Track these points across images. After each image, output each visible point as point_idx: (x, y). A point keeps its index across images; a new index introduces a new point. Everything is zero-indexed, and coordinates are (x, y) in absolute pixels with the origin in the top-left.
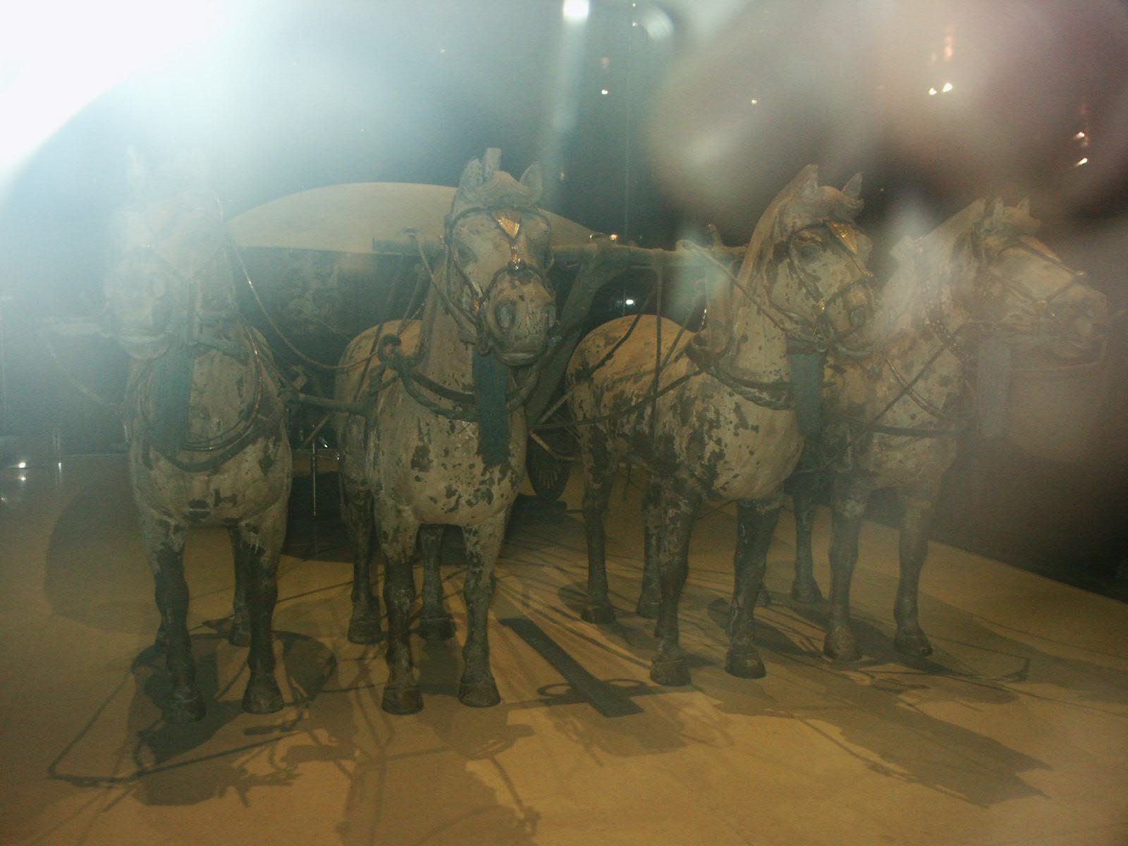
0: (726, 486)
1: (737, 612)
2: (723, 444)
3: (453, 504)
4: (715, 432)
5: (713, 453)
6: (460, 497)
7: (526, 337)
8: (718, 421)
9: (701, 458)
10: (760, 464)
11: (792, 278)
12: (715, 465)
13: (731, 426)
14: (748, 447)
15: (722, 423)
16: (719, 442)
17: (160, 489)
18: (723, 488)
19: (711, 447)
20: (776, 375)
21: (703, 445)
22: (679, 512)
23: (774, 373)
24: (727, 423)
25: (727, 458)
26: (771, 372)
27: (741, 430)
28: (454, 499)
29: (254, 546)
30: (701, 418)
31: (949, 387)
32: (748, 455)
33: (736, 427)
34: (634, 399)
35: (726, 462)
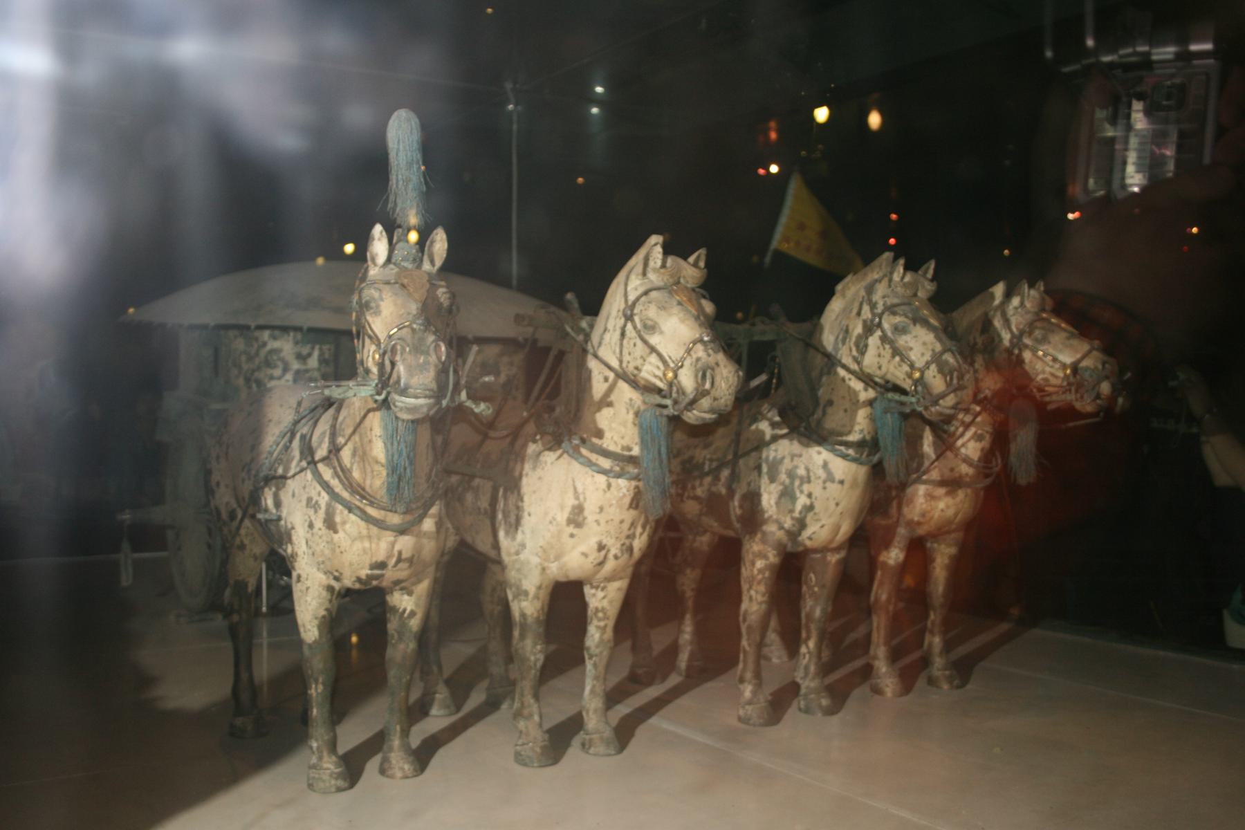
0: (813, 536)
1: (807, 656)
2: (814, 497)
3: (601, 558)
4: (806, 487)
6: (608, 551)
7: (721, 398)
9: (792, 511)
11: (884, 349)
12: (805, 517)
13: (820, 481)
16: (810, 495)
17: (342, 552)
18: (810, 538)
19: (802, 500)
21: (794, 499)
27: (828, 484)
28: (603, 553)
29: (404, 610)
30: (791, 475)
34: (707, 463)
35: (815, 514)
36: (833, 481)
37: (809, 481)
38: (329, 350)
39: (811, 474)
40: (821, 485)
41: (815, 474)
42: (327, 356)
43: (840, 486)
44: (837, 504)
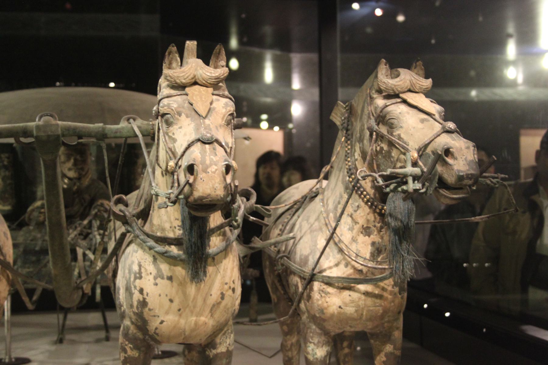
2: (145, 292)
5: (139, 301)
8: (140, 273)
10: (182, 310)
12: (142, 312)
13: (151, 277)
14: (167, 295)
15: (143, 275)
16: (141, 291)
20: (179, 230)
22: (126, 355)
23: (177, 228)
24: (148, 274)
25: (150, 305)
26: (175, 227)
27: (159, 280)
31: (372, 236)
32: (168, 303)
33: (155, 278)
35: (150, 310)
36: (163, 278)
37: (141, 278)
38: (8, 158)
39: (143, 270)
40: (152, 281)
41: (146, 270)
42: (6, 163)
43: (168, 282)
44: (171, 301)
